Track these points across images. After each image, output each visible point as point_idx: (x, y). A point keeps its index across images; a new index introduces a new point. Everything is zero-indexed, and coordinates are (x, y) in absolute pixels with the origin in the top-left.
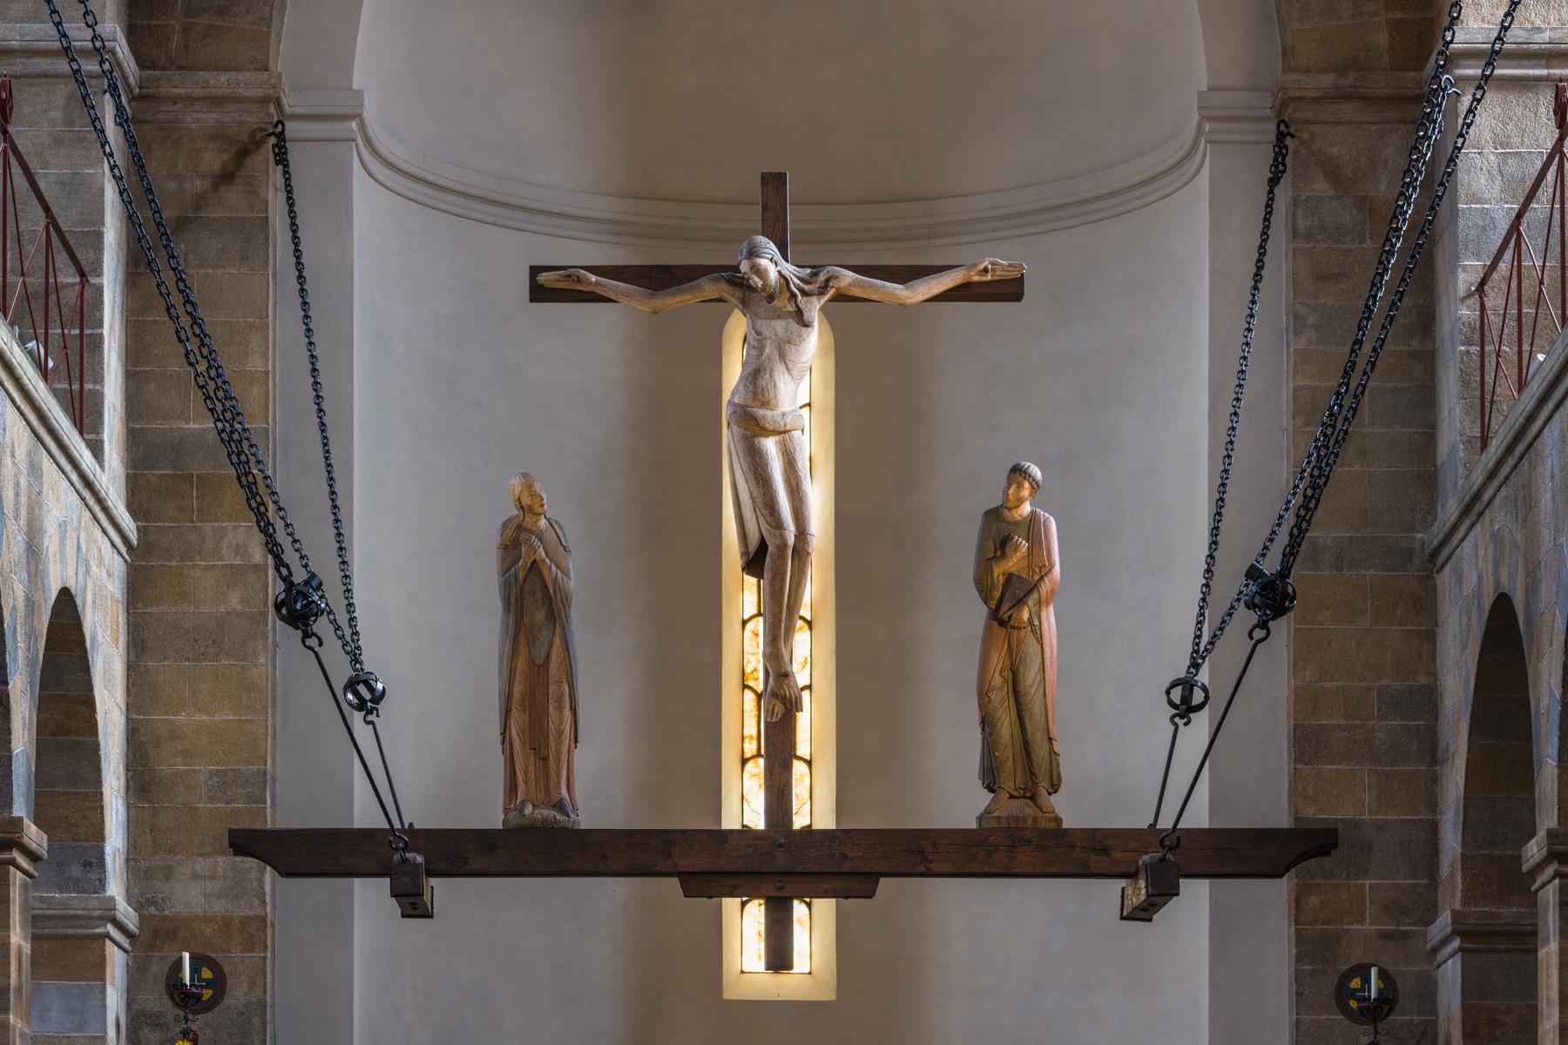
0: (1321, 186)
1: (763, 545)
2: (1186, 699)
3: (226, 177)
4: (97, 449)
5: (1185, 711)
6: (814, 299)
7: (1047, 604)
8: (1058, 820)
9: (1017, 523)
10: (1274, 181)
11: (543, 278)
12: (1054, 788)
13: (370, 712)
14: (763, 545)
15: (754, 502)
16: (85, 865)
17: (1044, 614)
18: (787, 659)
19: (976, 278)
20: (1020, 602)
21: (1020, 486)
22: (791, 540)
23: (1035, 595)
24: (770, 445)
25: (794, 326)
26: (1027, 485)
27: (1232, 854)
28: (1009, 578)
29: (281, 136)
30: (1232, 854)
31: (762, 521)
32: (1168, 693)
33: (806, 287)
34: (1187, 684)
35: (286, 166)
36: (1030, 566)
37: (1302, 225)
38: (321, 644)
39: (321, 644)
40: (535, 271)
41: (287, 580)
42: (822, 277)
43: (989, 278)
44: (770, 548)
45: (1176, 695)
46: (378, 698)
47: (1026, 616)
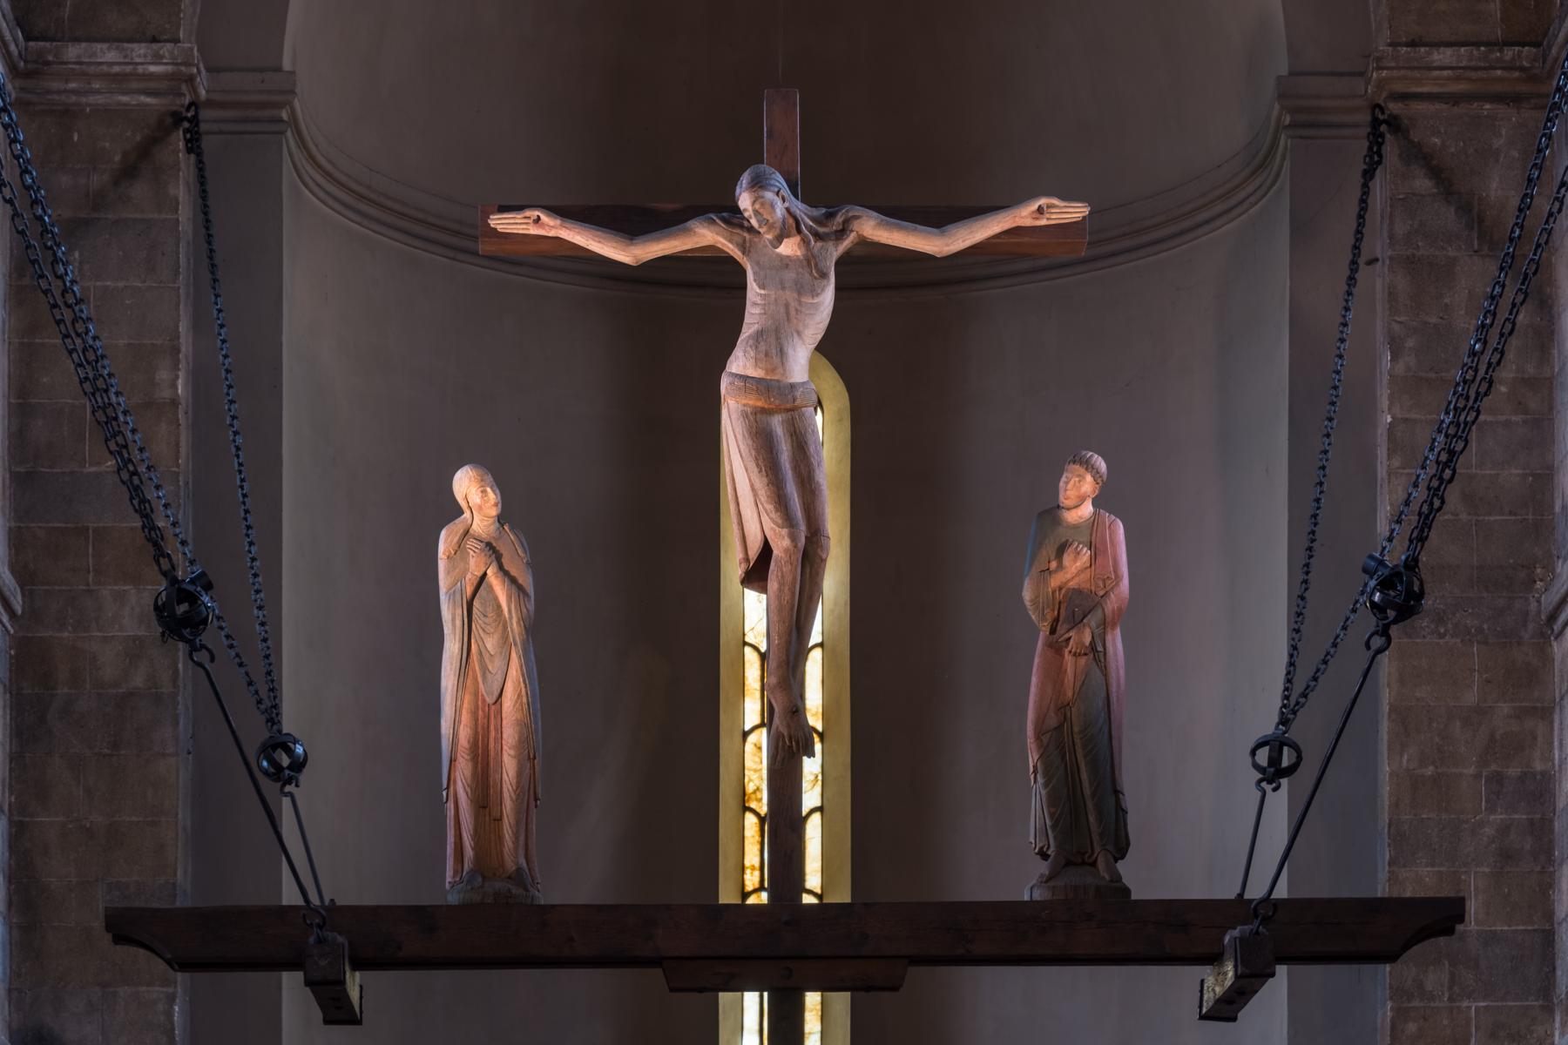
0: (1423, 183)
1: (766, 550)
2: (1275, 760)
3: (128, 173)
5: (1273, 774)
7: (1114, 626)
9: (1076, 527)
10: (1368, 174)
13: (289, 781)
14: (766, 550)
15: (755, 495)
17: (1109, 638)
23: (1098, 614)
26: (1089, 478)
29: (195, 121)
31: (765, 518)
32: (1253, 753)
34: (1275, 744)
35: (199, 155)
37: (1401, 229)
38: (212, 659)
39: (212, 659)
41: (169, 575)
44: (775, 552)
46: (298, 765)
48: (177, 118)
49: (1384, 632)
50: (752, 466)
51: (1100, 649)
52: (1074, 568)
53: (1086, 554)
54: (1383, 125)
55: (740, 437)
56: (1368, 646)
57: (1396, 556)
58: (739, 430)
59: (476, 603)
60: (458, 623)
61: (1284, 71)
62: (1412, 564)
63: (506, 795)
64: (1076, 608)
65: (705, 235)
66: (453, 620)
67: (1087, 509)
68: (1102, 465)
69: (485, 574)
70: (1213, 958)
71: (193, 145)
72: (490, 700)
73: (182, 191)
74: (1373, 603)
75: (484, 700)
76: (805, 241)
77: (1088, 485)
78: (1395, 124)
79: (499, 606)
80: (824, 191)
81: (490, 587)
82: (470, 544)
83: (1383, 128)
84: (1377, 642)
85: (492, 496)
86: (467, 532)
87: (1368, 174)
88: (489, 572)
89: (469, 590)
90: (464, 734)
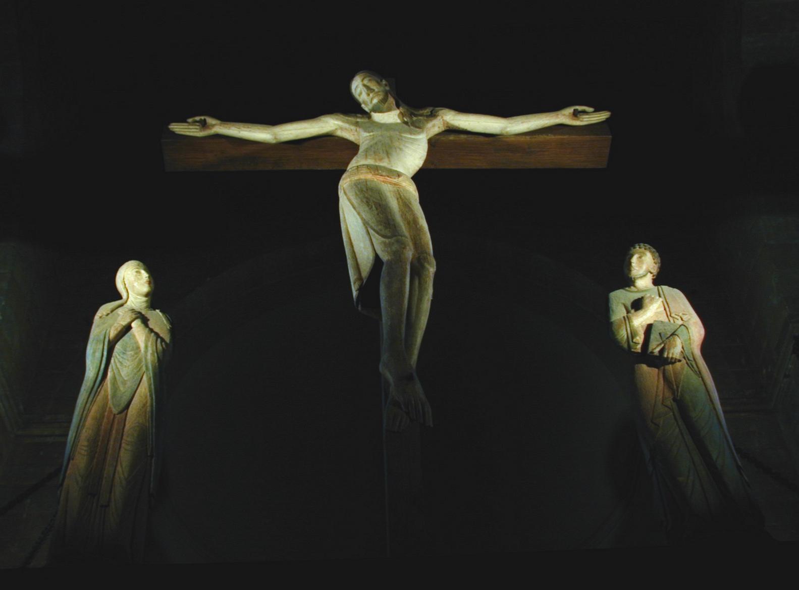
1: (377, 260)
28: (649, 328)
50: (364, 209)
55: (354, 201)
59: (118, 347)
65: (329, 124)
66: (94, 352)
69: (128, 328)
72: (115, 411)
75: (111, 411)
76: (402, 115)
79: (138, 348)
80: (416, 100)
85: (145, 275)
88: (133, 325)
89: (113, 333)
90: (86, 433)
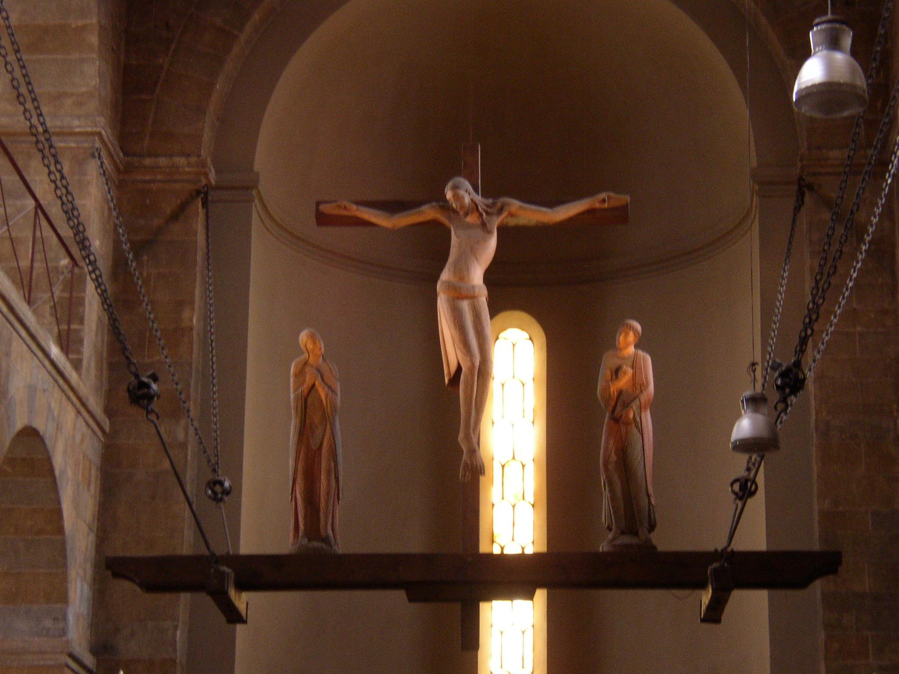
4: (77, 365)
6: (495, 218)
7: (645, 409)
8: (655, 548)
11: (325, 208)
12: (652, 527)
15: (453, 341)
16: (54, 620)
18: (475, 440)
19: (598, 205)
20: (627, 405)
21: (627, 335)
22: (477, 363)
24: (465, 305)
25: (480, 232)
26: (631, 334)
27: (771, 571)
28: (620, 393)
29: (206, 194)
30: (771, 571)
33: (489, 210)
36: (634, 385)
39: (158, 417)
40: (318, 204)
42: (499, 205)
43: (606, 205)
44: (464, 369)
45: (737, 487)
47: (631, 416)
48: (198, 192)
49: (784, 400)
51: (638, 420)
52: (624, 382)
53: (630, 371)
54: (803, 187)
56: (776, 408)
57: (788, 361)
58: (446, 310)
60: (299, 408)
61: (754, 163)
62: (798, 364)
63: (322, 496)
64: (624, 400)
67: (631, 350)
68: (638, 327)
69: (314, 385)
70: (702, 586)
71: (205, 204)
73: (200, 227)
74: (777, 386)
77: (631, 337)
78: (810, 187)
81: (317, 391)
82: (307, 369)
83: (806, 190)
84: (781, 406)
86: (306, 363)
87: (797, 210)
